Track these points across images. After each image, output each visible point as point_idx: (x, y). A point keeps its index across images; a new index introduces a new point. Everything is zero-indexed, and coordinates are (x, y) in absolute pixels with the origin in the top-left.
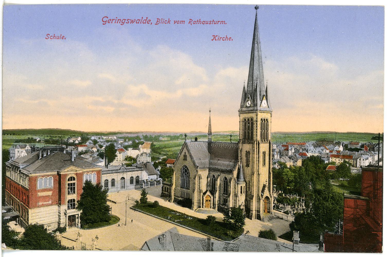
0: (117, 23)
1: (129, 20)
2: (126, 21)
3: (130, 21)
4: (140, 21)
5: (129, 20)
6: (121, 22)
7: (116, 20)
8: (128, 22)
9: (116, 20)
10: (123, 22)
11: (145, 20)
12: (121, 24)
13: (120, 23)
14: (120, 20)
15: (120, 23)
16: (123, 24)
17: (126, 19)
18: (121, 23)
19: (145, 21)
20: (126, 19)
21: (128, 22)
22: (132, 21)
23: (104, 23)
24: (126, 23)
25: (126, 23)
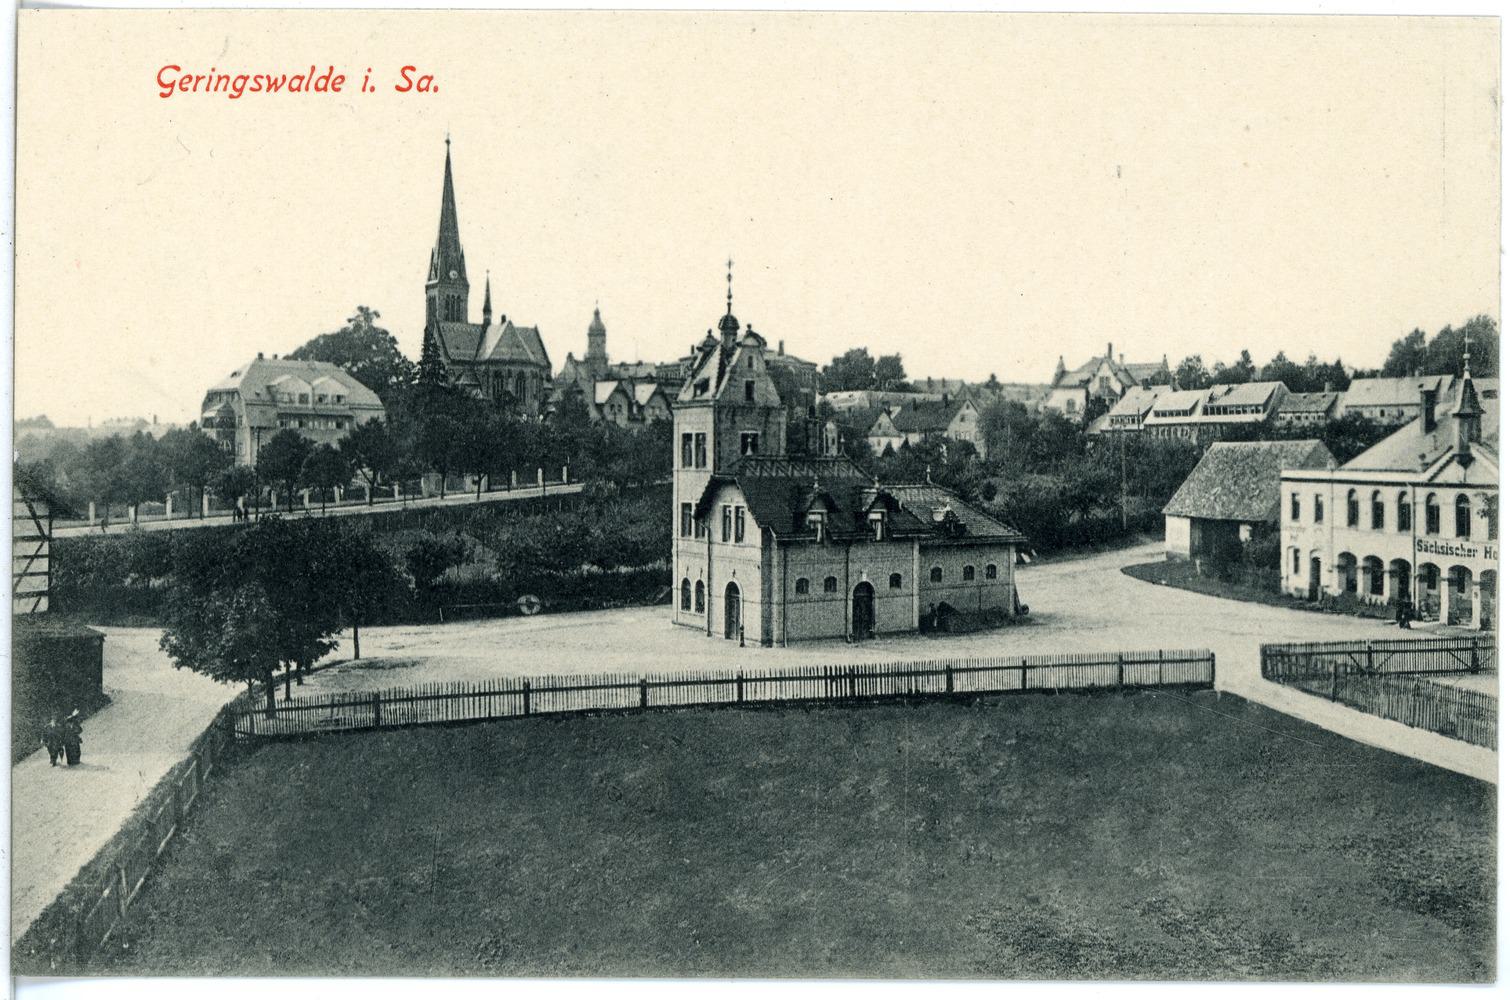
0: (216, 89)
1: (262, 77)
2: (251, 83)
3: (264, 83)
4: (305, 82)
5: (262, 77)
6: (230, 86)
7: (211, 78)
8: (256, 86)
9: (211, 78)
10: (239, 84)
11: (323, 77)
12: (231, 96)
13: (225, 89)
14: (228, 78)
15: (225, 89)
16: (236, 94)
17: (248, 77)
18: (230, 90)
19: (323, 81)
20: (248, 77)
21: (256, 86)
22: (272, 81)
23: (167, 89)
24: (252, 89)
25: (252, 89)
